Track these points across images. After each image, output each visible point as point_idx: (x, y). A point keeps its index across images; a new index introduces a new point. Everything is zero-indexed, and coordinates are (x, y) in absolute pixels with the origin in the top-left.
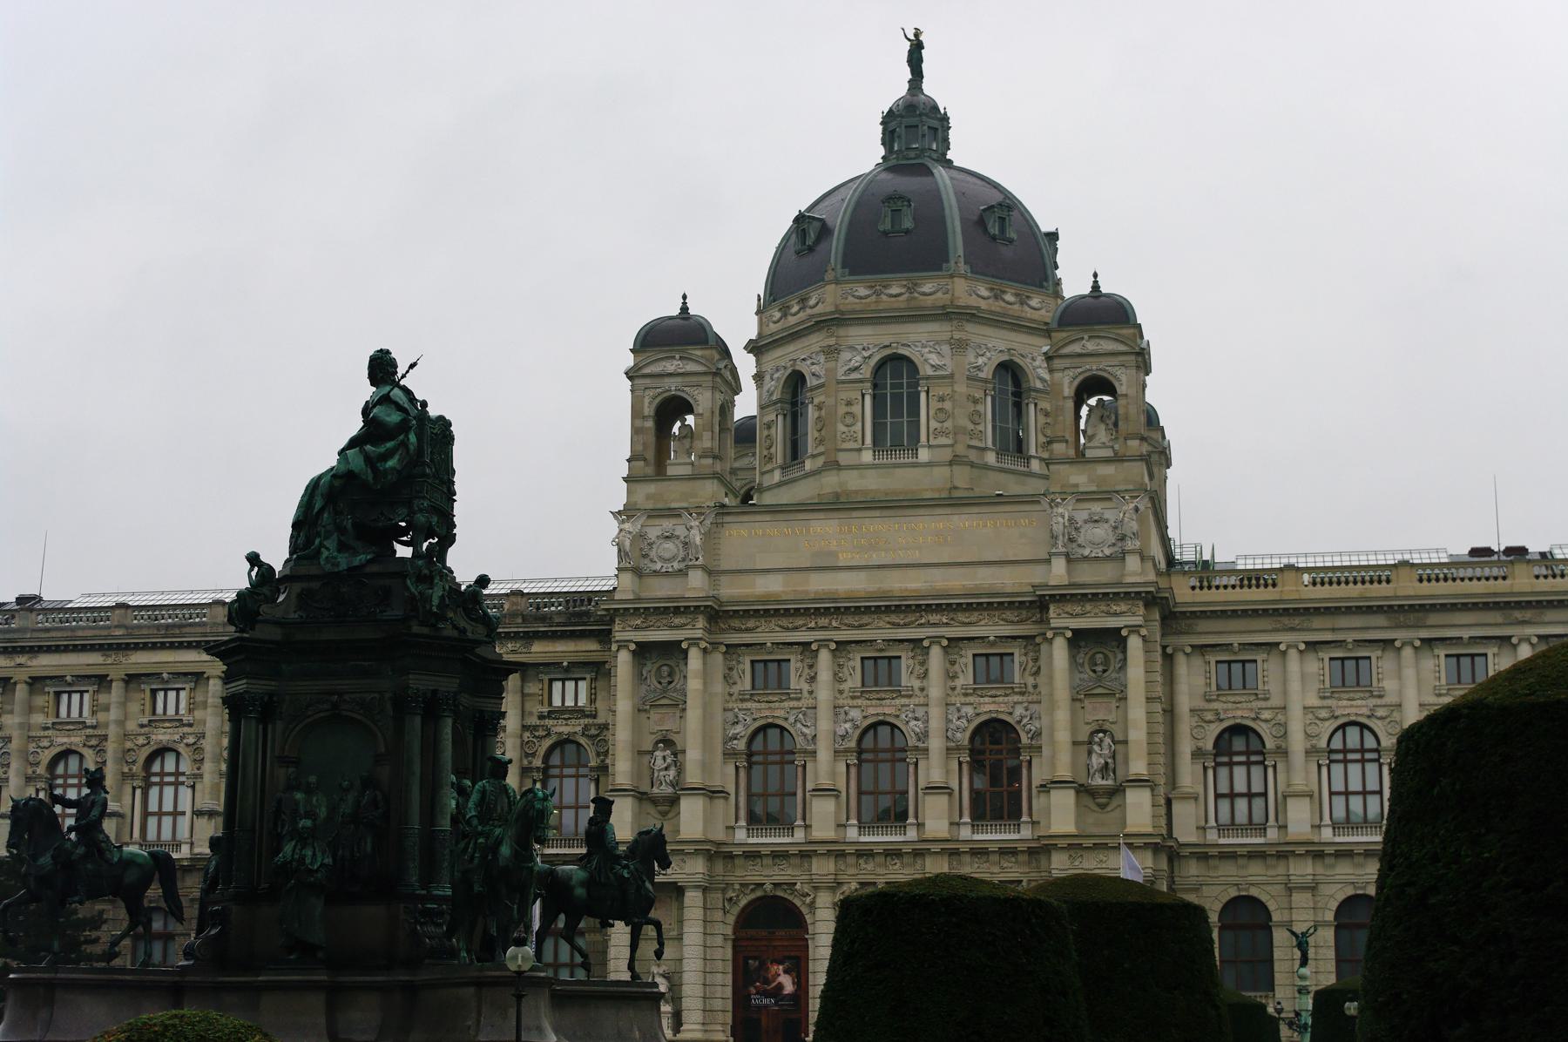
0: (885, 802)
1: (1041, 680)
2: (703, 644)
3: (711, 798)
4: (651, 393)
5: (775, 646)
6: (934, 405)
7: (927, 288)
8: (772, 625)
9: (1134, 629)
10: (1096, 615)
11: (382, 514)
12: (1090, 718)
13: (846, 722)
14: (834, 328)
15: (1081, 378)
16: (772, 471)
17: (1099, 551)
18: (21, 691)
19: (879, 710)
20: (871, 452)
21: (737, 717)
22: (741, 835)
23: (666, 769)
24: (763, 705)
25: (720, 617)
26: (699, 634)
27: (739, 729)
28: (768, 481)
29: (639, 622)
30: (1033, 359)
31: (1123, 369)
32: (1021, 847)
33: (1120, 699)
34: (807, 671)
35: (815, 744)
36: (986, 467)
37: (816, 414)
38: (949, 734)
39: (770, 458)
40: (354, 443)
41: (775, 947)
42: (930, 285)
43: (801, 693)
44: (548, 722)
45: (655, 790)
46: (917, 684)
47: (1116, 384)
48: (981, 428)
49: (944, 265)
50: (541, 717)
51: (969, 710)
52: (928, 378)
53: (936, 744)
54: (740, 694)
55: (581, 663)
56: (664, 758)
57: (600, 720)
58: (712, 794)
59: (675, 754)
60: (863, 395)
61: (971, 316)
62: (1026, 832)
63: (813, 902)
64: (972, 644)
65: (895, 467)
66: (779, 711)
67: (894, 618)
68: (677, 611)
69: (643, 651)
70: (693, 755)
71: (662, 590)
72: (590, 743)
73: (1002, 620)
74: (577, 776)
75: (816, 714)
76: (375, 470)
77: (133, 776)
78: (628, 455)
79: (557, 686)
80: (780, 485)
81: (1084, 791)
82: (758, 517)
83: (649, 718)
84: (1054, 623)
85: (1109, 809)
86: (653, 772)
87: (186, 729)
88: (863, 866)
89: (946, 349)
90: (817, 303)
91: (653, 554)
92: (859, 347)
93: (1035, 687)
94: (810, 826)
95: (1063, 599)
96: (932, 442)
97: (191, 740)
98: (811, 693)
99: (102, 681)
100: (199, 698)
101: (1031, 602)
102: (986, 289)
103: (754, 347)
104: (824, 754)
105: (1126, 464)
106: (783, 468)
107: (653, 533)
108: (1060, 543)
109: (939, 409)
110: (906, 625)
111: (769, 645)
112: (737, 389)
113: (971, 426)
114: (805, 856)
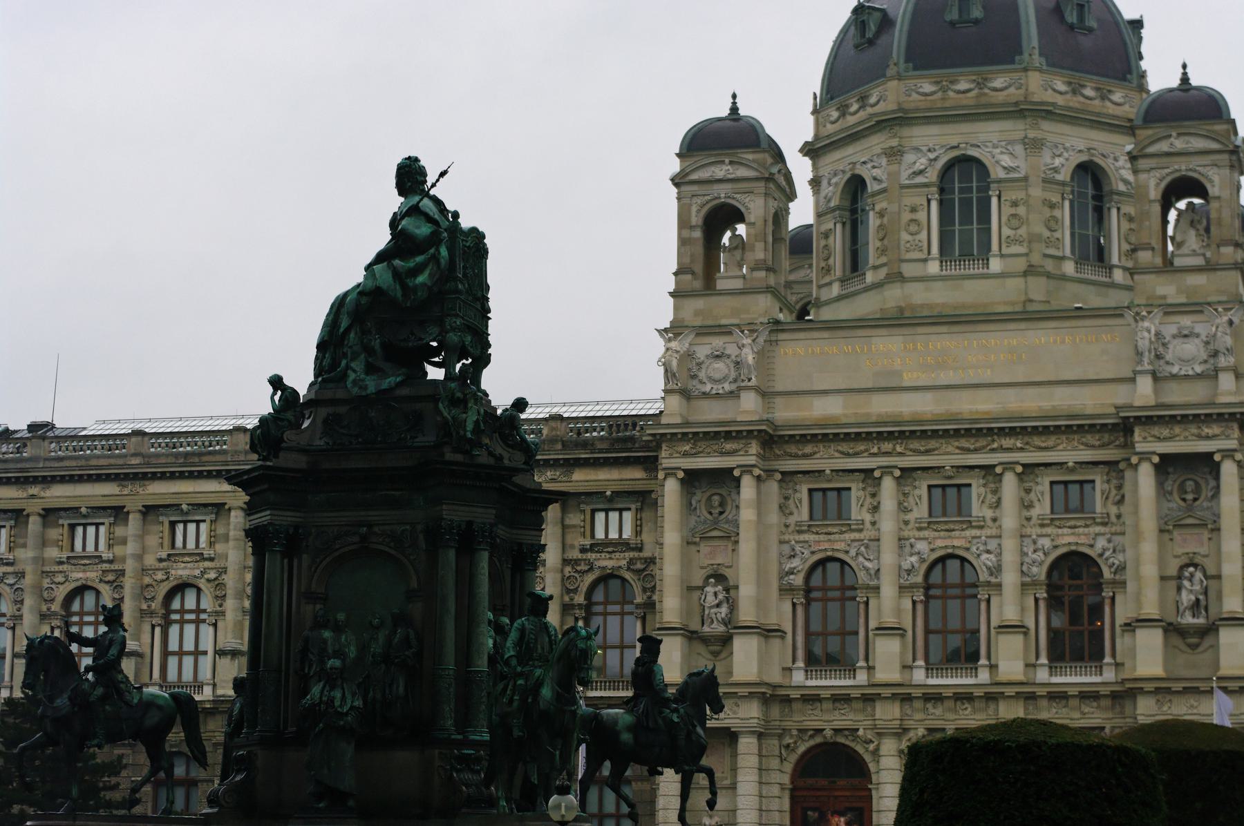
0: (955, 641)
1: (1126, 509)
2: (757, 472)
3: (766, 637)
4: (699, 201)
5: (834, 474)
6: (1007, 211)
7: (998, 83)
8: (831, 451)
9: (1228, 454)
10: (1186, 439)
11: (413, 334)
12: (1180, 551)
13: (911, 555)
14: (897, 128)
15: (1169, 179)
16: (829, 284)
17: (1189, 368)
18: (34, 524)
19: (948, 542)
20: (937, 263)
21: (793, 550)
22: (798, 677)
23: (718, 606)
24: (822, 537)
25: (775, 442)
26: (752, 460)
27: (795, 563)
28: (825, 295)
29: (687, 448)
30: (1116, 159)
31: (1215, 170)
32: (1104, 690)
33: (1212, 530)
34: (869, 500)
35: (878, 579)
36: (1064, 278)
37: (878, 222)
38: (1025, 568)
39: (828, 270)
40: (381, 257)
41: (836, 797)
42: (1002, 80)
43: (863, 524)
44: (591, 556)
45: (706, 629)
46: (989, 513)
47: (1208, 186)
48: (1058, 235)
49: (1017, 58)
50: (583, 550)
51: (1046, 543)
52: (1000, 181)
53: (1010, 578)
54: (796, 525)
55: (625, 492)
56: (716, 594)
57: (646, 554)
58: (767, 633)
59: (727, 590)
60: (929, 201)
61: (1047, 113)
62: (1109, 675)
63: (877, 749)
64: (1049, 471)
65: (964, 279)
66: (839, 544)
67: (964, 443)
68: (728, 436)
69: (692, 479)
70: (746, 591)
71: (711, 413)
72: (636, 578)
73: (1082, 444)
74: (622, 614)
75: (879, 546)
76: (404, 287)
77: (151, 613)
78: (674, 268)
79: (600, 517)
80: (839, 298)
81: (1172, 630)
82: (816, 334)
83: (699, 551)
84: (1140, 447)
85: (1201, 649)
86: (704, 610)
87: (207, 564)
88: (931, 710)
89: (1019, 149)
90: (878, 102)
91: (702, 375)
92: (925, 149)
93: (1119, 516)
94: (874, 668)
95: (1149, 421)
96: (1005, 251)
97: (212, 575)
98: (873, 524)
99: (118, 513)
100: (221, 530)
101: (1113, 425)
102: (1064, 83)
103: (809, 150)
104: (888, 590)
105: (1219, 273)
106: (843, 281)
107: (702, 352)
108: (1146, 360)
109: (1012, 215)
110: (976, 450)
111: (828, 472)
112: (791, 195)
113: (1047, 233)
114: (869, 699)
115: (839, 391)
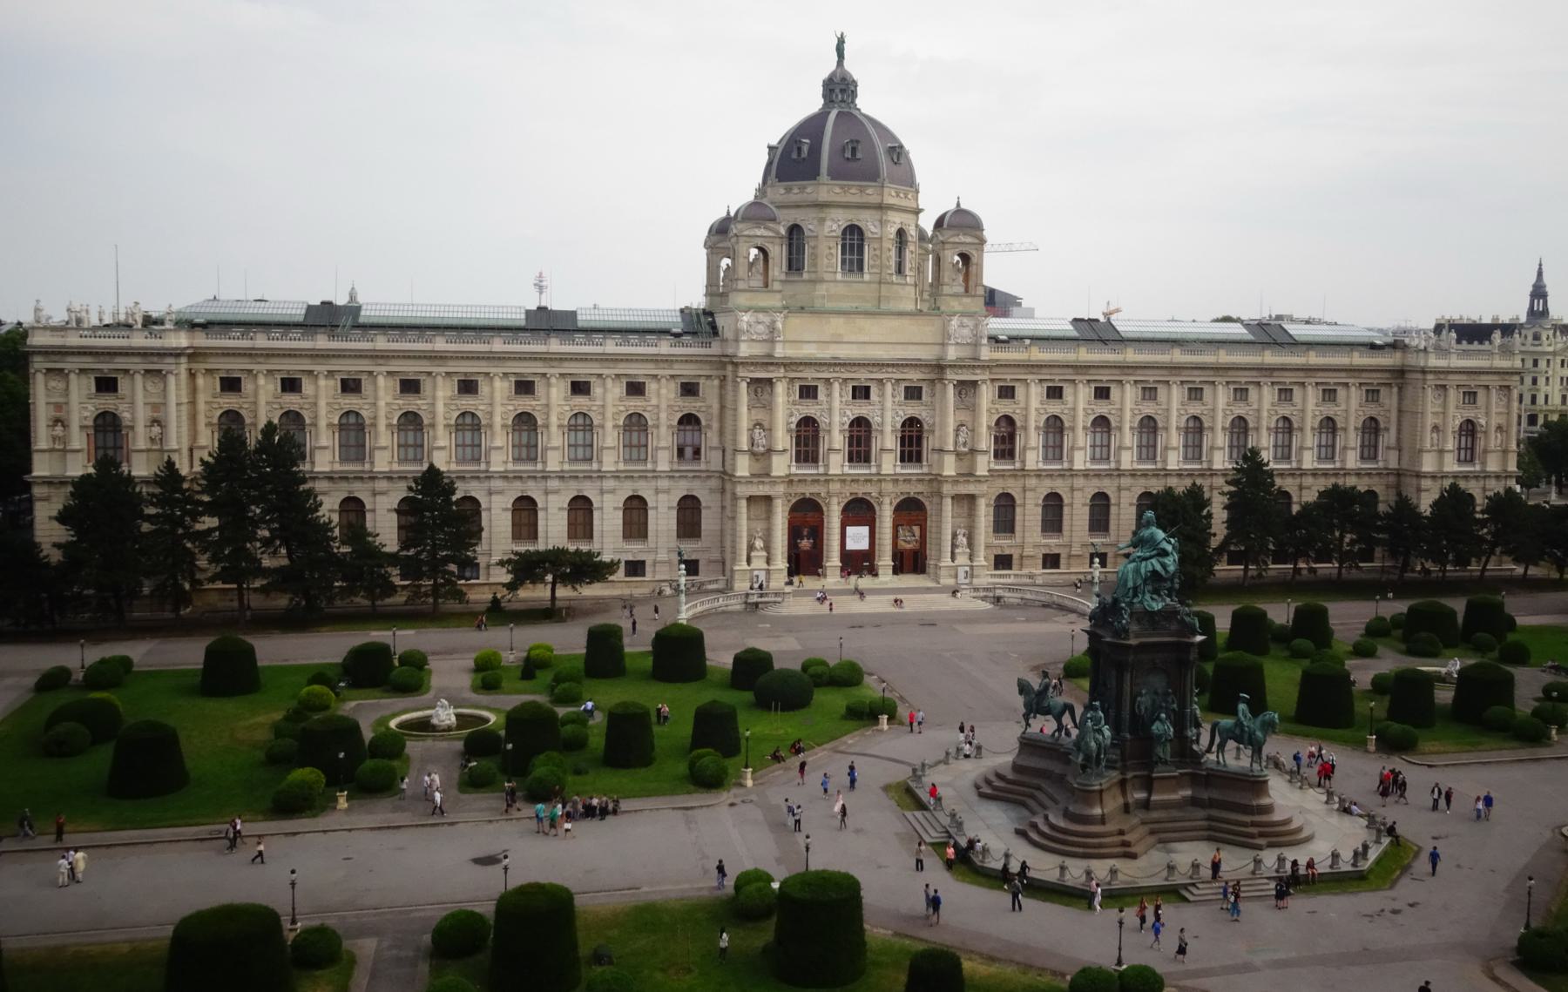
7: (869, 191)
26: (782, 375)
36: (892, 283)
53: (888, 429)
89: (877, 223)
96: (871, 271)
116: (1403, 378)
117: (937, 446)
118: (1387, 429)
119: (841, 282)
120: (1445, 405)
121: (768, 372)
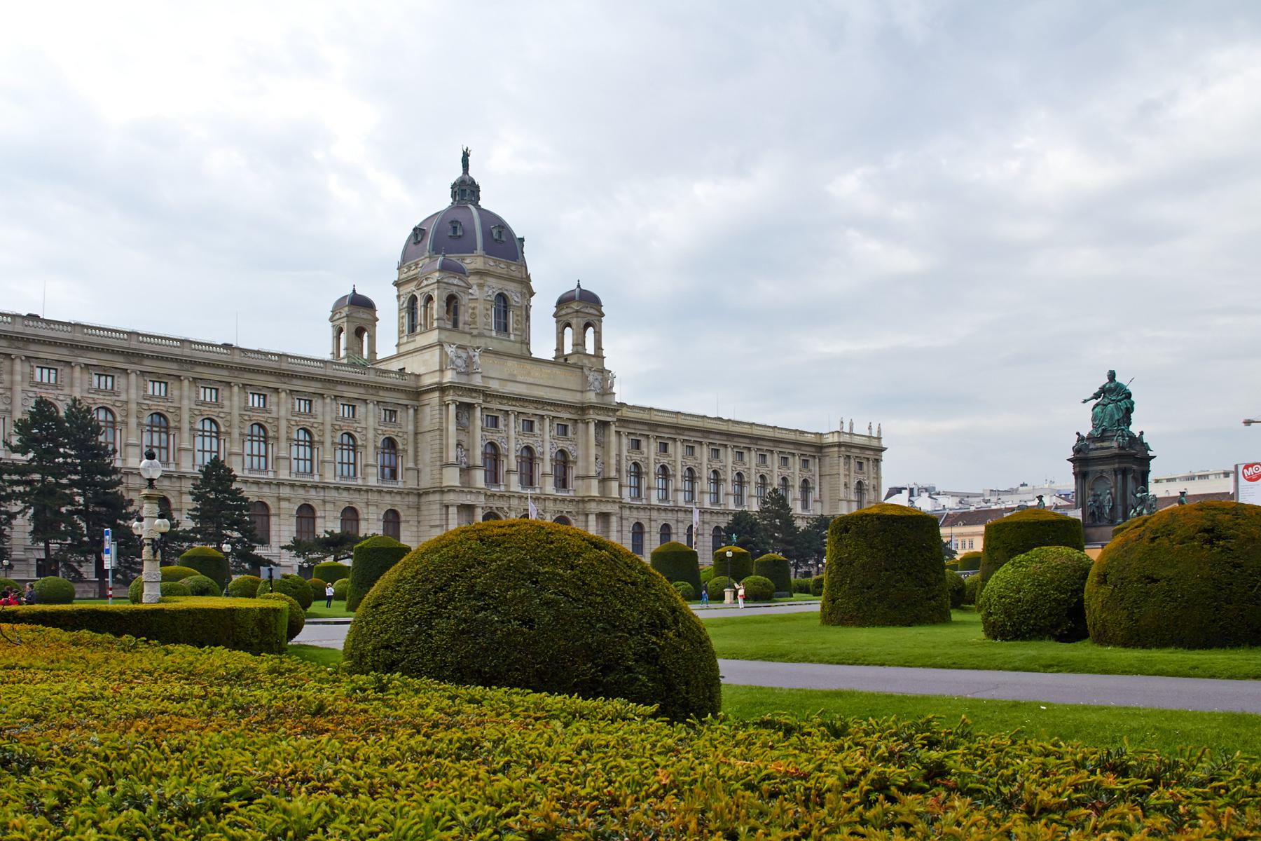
4: (447, 291)
26: (481, 401)
53: (547, 457)
66: (495, 438)
67: (535, 405)
95: (594, 407)
115: (498, 379)
116: (821, 452)
117: (582, 473)
118: (814, 488)
119: (494, 338)
120: (849, 470)
121: (472, 397)
